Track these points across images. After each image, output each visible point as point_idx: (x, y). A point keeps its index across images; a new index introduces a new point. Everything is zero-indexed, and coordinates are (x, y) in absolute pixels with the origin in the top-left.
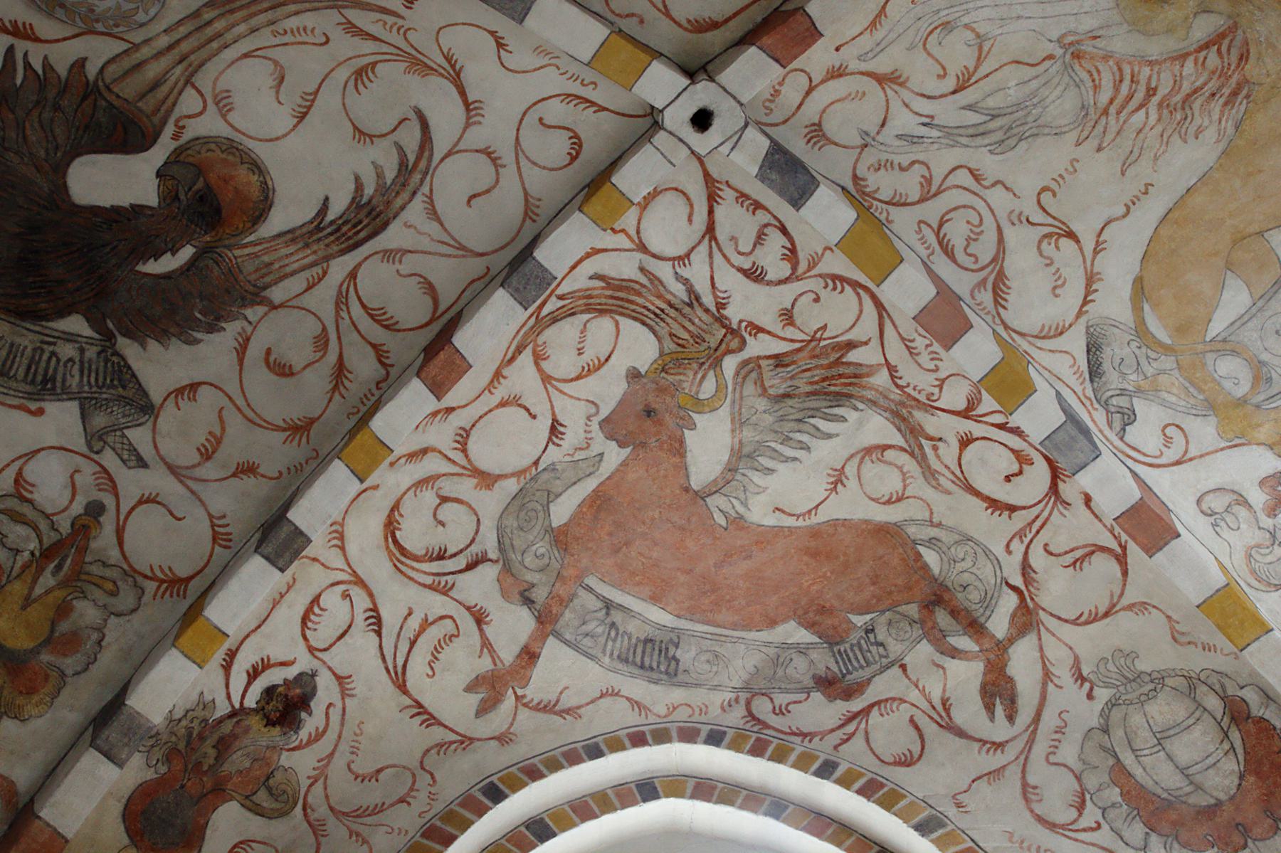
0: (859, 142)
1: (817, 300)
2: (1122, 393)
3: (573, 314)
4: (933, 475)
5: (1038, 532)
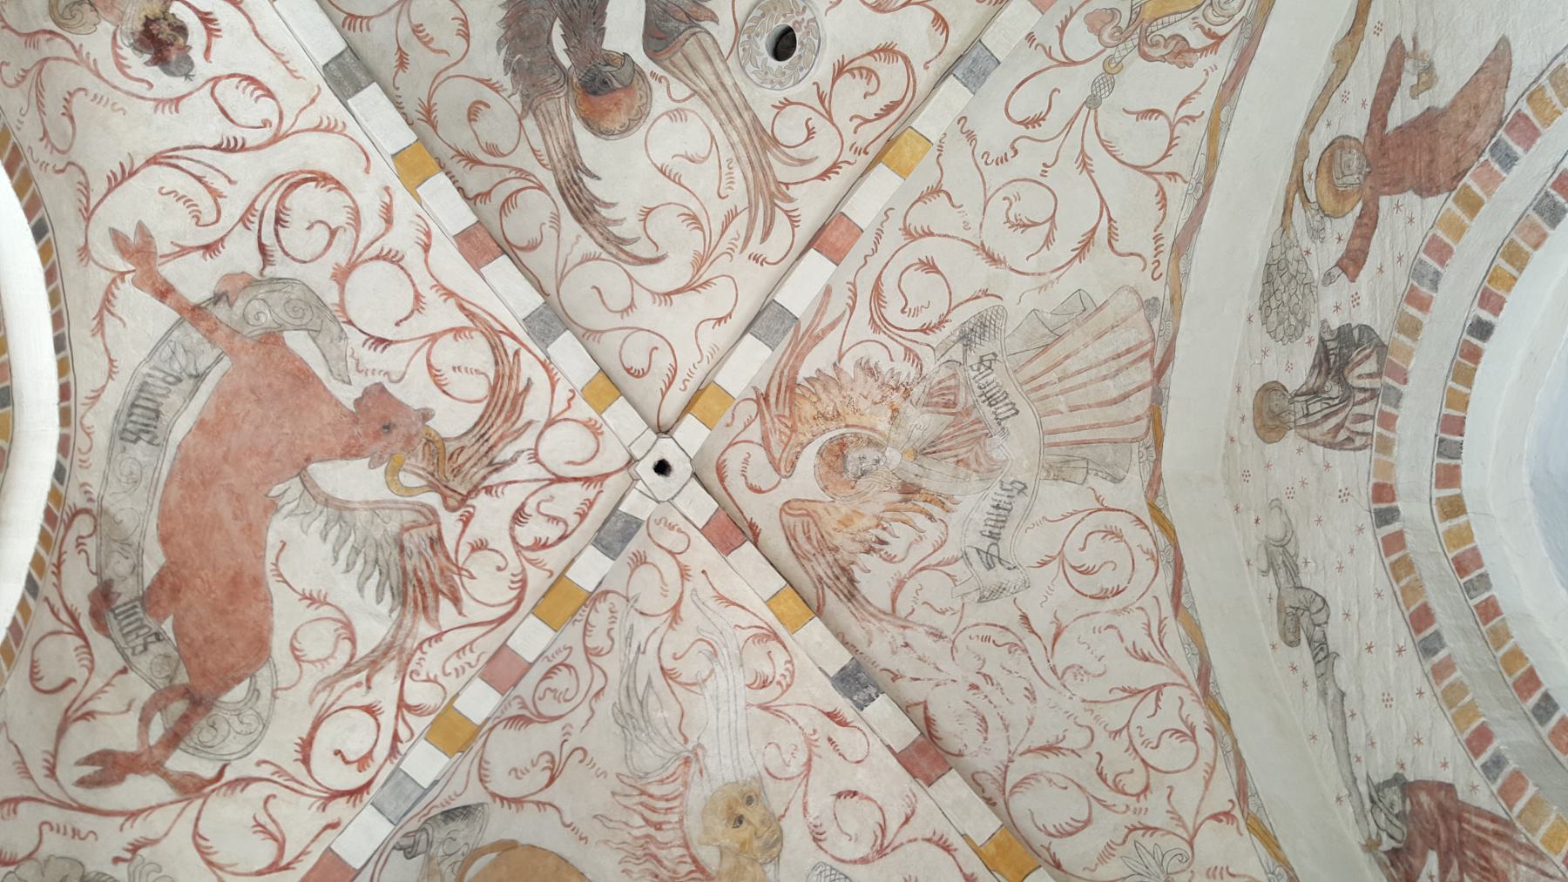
0: (631, 595)
1: (499, 569)
2: (429, 844)
3: (497, 363)
4: (328, 686)
5: (287, 787)
